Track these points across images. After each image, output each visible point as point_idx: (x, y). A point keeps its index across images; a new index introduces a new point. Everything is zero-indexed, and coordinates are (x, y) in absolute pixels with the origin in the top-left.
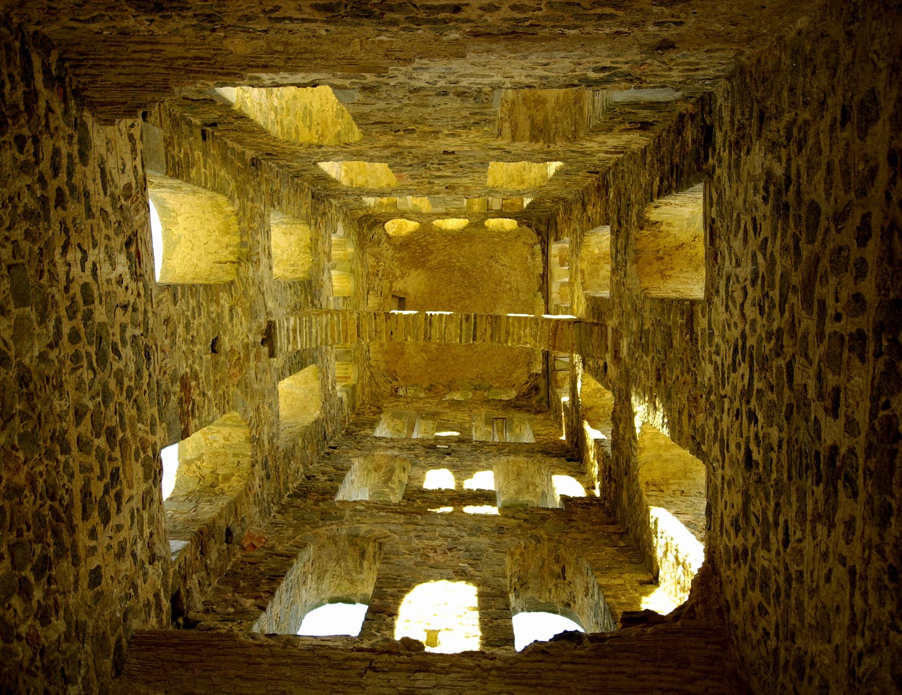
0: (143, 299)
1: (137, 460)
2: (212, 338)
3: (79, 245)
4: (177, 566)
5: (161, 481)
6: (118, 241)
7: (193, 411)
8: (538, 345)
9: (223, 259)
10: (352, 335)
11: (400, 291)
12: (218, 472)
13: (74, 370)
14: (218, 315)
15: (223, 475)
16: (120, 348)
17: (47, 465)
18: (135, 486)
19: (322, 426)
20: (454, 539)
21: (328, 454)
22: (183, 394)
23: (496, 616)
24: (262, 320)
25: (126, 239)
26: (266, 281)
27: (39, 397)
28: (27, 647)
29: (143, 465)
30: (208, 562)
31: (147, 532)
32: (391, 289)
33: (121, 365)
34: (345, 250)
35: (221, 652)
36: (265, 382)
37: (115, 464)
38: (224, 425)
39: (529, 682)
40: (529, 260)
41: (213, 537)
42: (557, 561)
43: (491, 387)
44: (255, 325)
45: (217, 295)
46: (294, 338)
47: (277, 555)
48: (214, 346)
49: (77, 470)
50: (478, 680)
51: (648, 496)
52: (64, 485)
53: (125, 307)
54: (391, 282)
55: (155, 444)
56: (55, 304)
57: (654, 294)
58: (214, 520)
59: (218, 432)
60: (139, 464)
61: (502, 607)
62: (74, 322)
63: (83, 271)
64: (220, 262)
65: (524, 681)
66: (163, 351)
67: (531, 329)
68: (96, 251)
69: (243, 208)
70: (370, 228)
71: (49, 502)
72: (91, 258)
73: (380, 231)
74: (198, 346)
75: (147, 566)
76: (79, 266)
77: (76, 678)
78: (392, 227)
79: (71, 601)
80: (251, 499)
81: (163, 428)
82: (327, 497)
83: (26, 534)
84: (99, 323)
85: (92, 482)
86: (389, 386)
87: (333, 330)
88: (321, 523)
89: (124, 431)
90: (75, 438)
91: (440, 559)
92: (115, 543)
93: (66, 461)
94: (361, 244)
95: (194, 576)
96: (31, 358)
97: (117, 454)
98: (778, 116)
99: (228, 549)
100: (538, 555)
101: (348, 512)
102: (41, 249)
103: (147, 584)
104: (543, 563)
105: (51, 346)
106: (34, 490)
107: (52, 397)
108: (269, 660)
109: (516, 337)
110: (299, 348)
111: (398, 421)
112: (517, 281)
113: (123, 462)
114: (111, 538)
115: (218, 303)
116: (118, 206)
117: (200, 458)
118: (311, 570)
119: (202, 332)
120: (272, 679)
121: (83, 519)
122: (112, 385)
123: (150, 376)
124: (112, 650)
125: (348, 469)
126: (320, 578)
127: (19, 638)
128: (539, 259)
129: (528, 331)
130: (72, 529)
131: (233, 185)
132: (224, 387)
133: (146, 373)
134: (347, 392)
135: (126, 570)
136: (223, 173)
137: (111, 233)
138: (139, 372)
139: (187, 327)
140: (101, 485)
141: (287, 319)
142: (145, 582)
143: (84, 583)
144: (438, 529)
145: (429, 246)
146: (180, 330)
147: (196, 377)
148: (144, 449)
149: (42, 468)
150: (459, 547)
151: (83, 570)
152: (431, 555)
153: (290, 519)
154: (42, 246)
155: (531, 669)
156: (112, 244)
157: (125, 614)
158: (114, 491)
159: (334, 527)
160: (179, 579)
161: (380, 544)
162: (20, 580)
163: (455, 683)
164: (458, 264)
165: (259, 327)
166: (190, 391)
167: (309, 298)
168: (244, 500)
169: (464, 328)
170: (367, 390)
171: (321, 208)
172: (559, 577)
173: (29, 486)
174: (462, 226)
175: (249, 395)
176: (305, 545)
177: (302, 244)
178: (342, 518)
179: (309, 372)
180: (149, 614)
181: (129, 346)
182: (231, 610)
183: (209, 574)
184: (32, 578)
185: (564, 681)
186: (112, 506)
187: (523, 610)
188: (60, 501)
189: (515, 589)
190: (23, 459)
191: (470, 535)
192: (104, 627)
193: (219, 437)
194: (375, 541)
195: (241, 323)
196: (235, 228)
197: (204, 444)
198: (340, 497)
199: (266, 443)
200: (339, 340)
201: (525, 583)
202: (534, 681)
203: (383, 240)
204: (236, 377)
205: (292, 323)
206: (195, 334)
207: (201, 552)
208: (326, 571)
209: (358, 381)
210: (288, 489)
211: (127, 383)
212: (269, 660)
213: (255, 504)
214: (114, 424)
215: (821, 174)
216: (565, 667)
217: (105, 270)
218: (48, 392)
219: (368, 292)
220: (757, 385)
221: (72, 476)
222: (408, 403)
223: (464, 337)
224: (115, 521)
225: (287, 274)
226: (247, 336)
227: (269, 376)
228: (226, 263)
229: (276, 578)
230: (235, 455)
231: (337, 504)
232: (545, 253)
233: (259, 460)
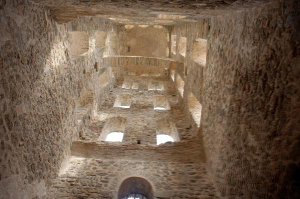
20: (144, 118)
57: (195, 61)
70: (120, 27)
78: (126, 27)
94: (118, 33)
97: (67, 103)
98: (222, 33)
126: (111, 127)
128: (168, 37)
130: (61, 121)
151: (63, 130)
215: (228, 51)
220: (213, 92)
224: (68, 118)
232: (170, 36)
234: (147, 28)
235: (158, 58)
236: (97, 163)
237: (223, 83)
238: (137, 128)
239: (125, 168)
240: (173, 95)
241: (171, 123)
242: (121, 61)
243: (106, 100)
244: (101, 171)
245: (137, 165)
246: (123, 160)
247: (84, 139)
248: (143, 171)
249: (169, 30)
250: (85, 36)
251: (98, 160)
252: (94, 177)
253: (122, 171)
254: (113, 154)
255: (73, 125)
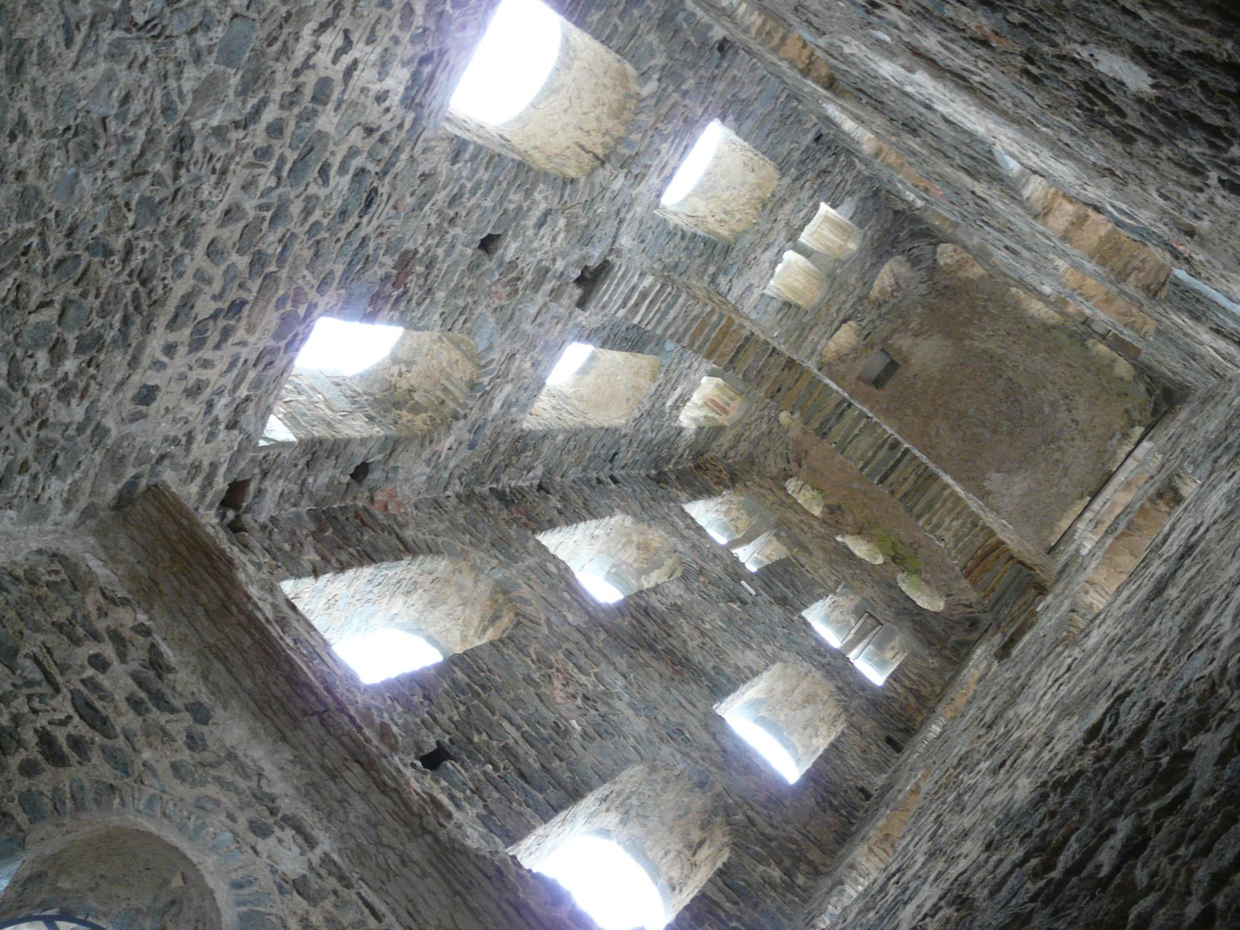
0: (403, 134)
1: (277, 308)
2: (489, 231)
3: (346, 33)
4: (262, 455)
5: (297, 350)
6: (406, 50)
7: (397, 301)
8: (953, 553)
9: (588, 146)
10: (722, 355)
11: (899, 351)
12: (415, 395)
13: (251, 165)
14: (520, 208)
15: (417, 403)
16: (332, 172)
17: (156, 246)
18: (257, 335)
19: (617, 442)
20: (608, 693)
21: (599, 481)
22: (394, 272)
23: (531, 802)
24: (597, 254)
25: (425, 53)
26: (639, 209)
27: (188, 171)
28: (29, 407)
29: (283, 318)
30: (311, 480)
31: (243, 392)
32: (887, 338)
33: (323, 192)
34: (846, 241)
35: (210, 570)
36: (546, 333)
37: (244, 295)
38: (457, 345)
39: (454, 882)
40: (1114, 441)
41: (337, 457)
42: (703, 828)
43: (916, 572)
44: (576, 255)
45: (534, 186)
46: (637, 305)
47: (399, 538)
48: (488, 244)
49: (190, 272)
50: (407, 830)
51: (871, 850)
52: (164, 279)
53: (369, 131)
54: (894, 331)
55: (316, 306)
56: (270, 82)
58: (348, 442)
59: (449, 351)
60: (277, 315)
61: (553, 802)
62: (285, 114)
63: (335, 61)
64: (582, 147)
65: (449, 877)
66: (395, 207)
67: (963, 525)
68: (369, 49)
69: (659, 98)
70: (913, 235)
71: (137, 284)
72: (354, 53)
73: (929, 249)
74: (458, 230)
75: (222, 427)
76: (332, 55)
77: (66, 475)
79: (105, 396)
80: (426, 454)
81: (339, 295)
82: (533, 526)
83: (91, 298)
84: (320, 132)
85: (203, 296)
86: (782, 465)
87: (700, 330)
88: (487, 545)
89: (280, 267)
90: (210, 238)
91: (559, 696)
92: (193, 377)
93: (182, 255)
95: (281, 482)
96: (204, 125)
97: (255, 286)
99: (348, 484)
100: (686, 799)
101: (531, 561)
102: (289, 14)
103: (209, 446)
104: (686, 814)
105: (237, 125)
106: (126, 260)
107: (205, 179)
108: (242, 618)
109: (935, 520)
110: (636, 321)
111: (745, 517)
112: (1076, 457)
113: (256, 299)
114: (191, 368)
115: (528, 194)
116: (438, 9)
117: (410, 363)
118: (427, 586)
119: (475, 216)
120: (228, 638)
121: (167, 327)
122: (296, 209)
123: (357, 226)
124: (124, 481)
125: (594, 514)
126: (433, 603)
127: (25, 392)
129: (956, 524)
130: (147, 329)
131: (660, 60)
132: (470, 300)
133: (354, 220)
134: (700, 429)
135: (190, 414)
136: (652, 38)
137: (405, 37)
138: (343, 214)
139: (454, 200)
140: (214, 306)
141: (642, 275)
142: (207, 442)
143: (131, 391)
144: (603, 666)
145: (986, 319)
146: (441, 197)
147: (430, 266)
148: (296, 303)
149: (148, 245)
150: (598, 705)
151: (137, 379)
152: (557, 684)
153: (460, 514)
154: (294, 11)
155: (469, 873)
156: (399, 50)
157: (162, 458)
158: (225, 323)
159: (496, 561)
160: (257, 471)
161: (519, 623)
162: (58, 339)
163: (381, 809)
164: (1011, 374)
165: (584, 259)
166: (407, 275)
167: (712, 269)
168: (414, 447)
169: (880, 455)
170: (743, 447)
171: (825, 162)
172: (690, 846)
173: (122, 254)
174: (1052, 322)
175: (508, 333)
176: (439, 553)
177: (758, 193)
178: (516, 561)
179: (643, 361)
180: (193, 479)
181: (348, 177)
182: (287, 547)
183: (301, 493)
184: (72, 346)
185: (489, 919)
186: (213, 337)
187: (619, 843)
188: (151, 291)
189: (626, 812)
190: (131, 223)
191: (632, 706)
192: (127, 450)
193: (444, 357)
194: (517, 614)
195: (554, 239)
196: (627, 115)
197: (424, 351)
198: (551, 540)
199: (497, 404)
200: (700, 348)
201: (646, 817)
202: (459, 887)
203: (923, 265)
204: (500, 298)
205: (647, 282)
206: (464, 213)
207: (308, 464)
208: (444, 602)
209: (734, 426)
210: (498, 480)
211: (317, 215)
212: (242, 618)
213: (428, 465)
214: (270, 251)
216: (505, 906)
217: (364, 76)
218: (203, 171)
219: (845, 321)
221: (181, 275)
222: (782, 504)
223: (871, 466)
224: (207, 353)
225: (711, 220)
226: (554, 260)
227: (560, 326)
228: (588, 152)
229: (368, 557)
230: (445, 389)
231: (531, 544)
233: (472, 418)
234: (1048, 328)
235: (947, 479)
236: (137, 654)
237: (1029, 754)
238: (517, 703)
239: (212, 790)
240: (897, 737)
241: (720, 836)
242: (748, 359)
243: (540, 487)
244: (105, 696)
245: (289, 832)
246: (258, 754)
247: (235, 528)
248: (266, 881)
249: (1155, 412)
250: (628, 96)
251: (164, 647)
252: (45, 689)
253: (183, 790)
254: (248, 683)
255: (222, 410)
